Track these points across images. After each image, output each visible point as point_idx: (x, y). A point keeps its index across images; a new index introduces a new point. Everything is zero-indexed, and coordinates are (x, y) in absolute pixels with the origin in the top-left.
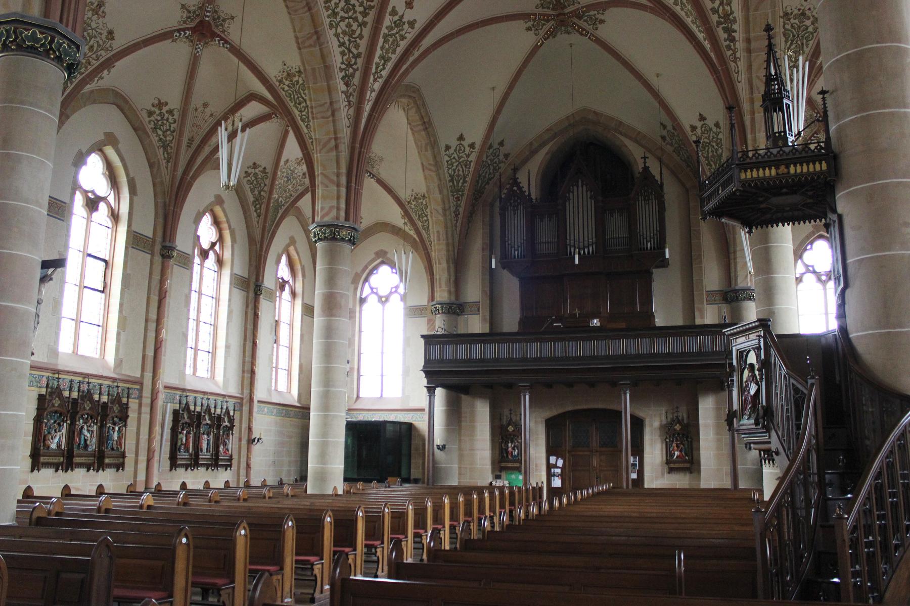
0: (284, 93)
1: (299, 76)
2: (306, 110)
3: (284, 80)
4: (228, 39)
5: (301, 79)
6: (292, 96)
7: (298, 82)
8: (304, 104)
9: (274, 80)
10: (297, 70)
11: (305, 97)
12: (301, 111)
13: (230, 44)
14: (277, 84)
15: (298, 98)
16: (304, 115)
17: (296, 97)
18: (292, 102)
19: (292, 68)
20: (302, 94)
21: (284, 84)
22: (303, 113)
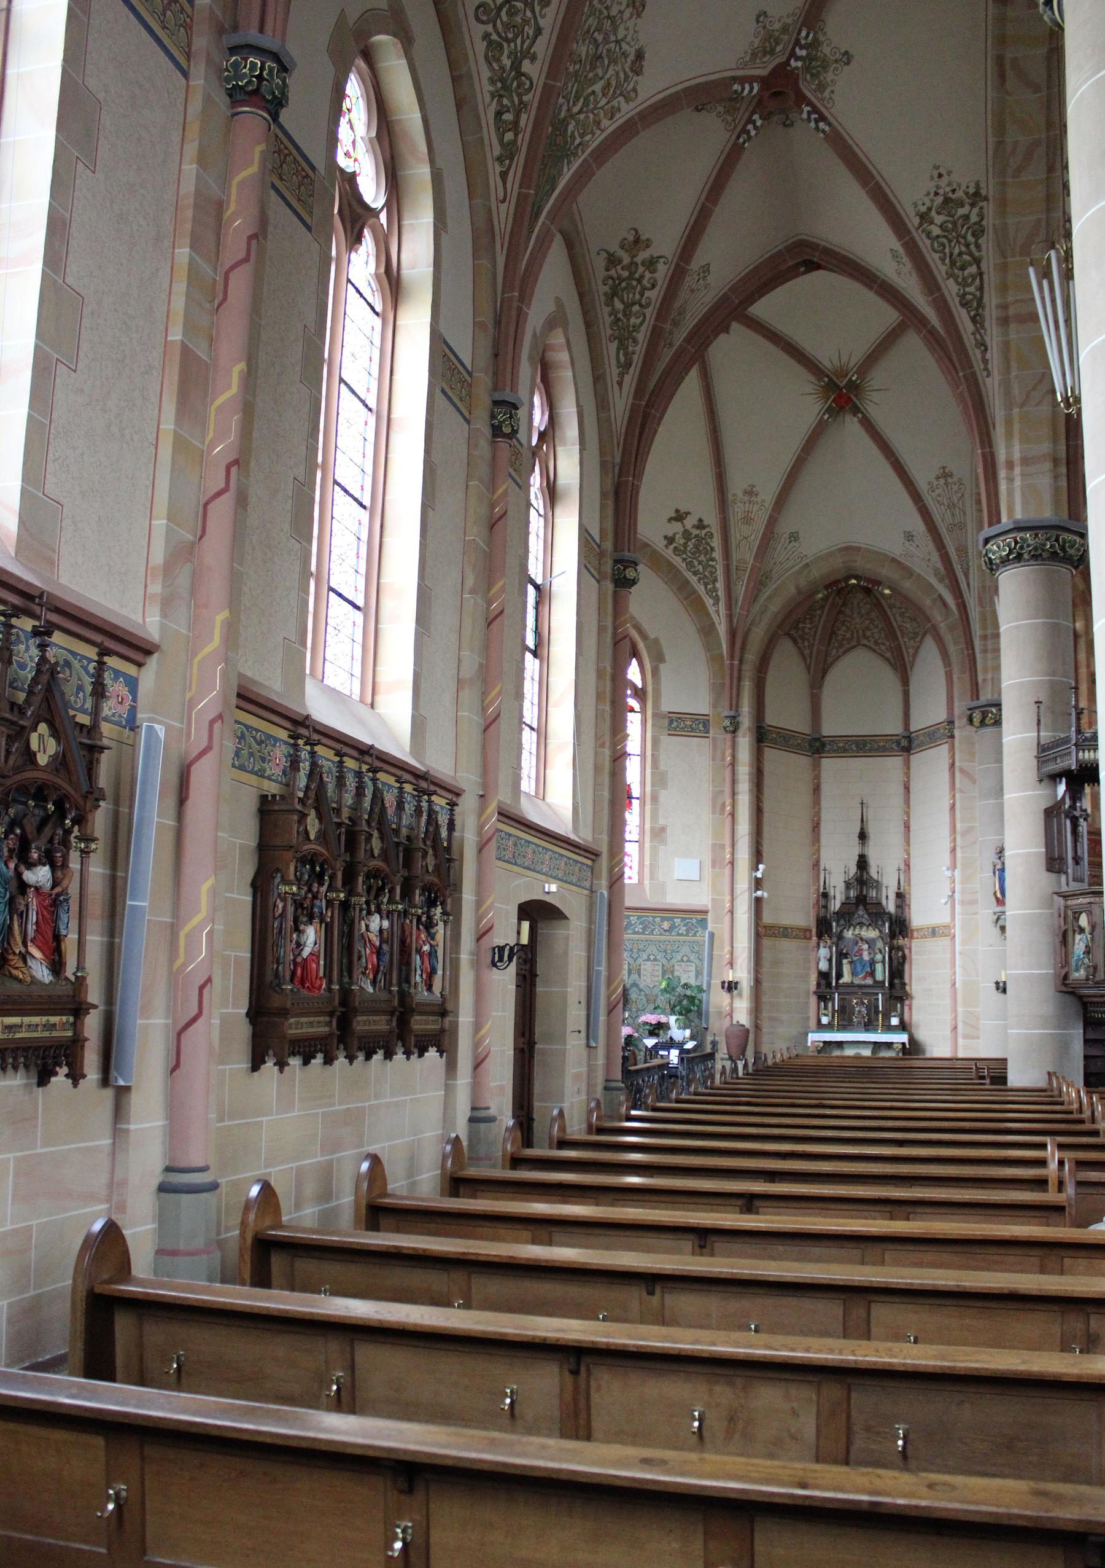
0: (928, 242)
1: (973, 205)
2: (978, 281)
3: (933, 213)
4: (826, 114)
5: (975, 210)
6: (947, 251)
7: (967, 217)
8: (973, 269)
9: (911, 212)
10: (972, 190)
11: (977, 254)
12: (964, 284)
13: (830, 124)
14: (917, 221)
15: (960, 254)
16: (969, 293)
17: (956, 251)
18: (944, 263)
19: (959, 185)
20: (972, 247)
21: (931, 223)
22: (967, 289)
